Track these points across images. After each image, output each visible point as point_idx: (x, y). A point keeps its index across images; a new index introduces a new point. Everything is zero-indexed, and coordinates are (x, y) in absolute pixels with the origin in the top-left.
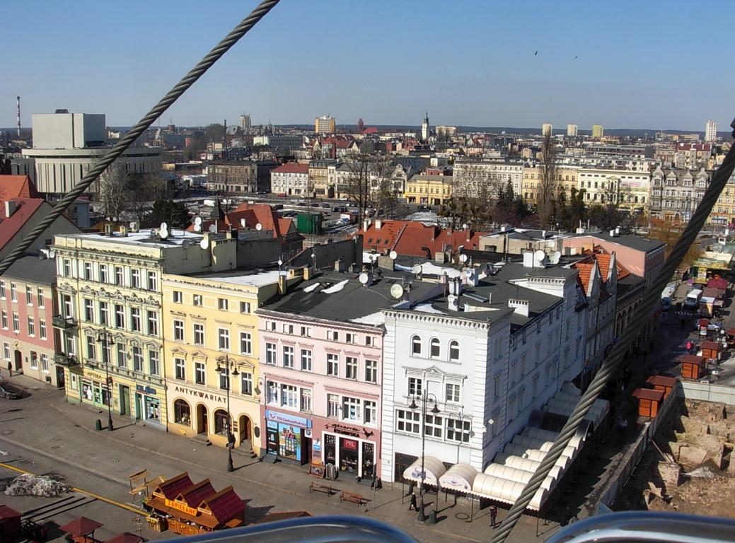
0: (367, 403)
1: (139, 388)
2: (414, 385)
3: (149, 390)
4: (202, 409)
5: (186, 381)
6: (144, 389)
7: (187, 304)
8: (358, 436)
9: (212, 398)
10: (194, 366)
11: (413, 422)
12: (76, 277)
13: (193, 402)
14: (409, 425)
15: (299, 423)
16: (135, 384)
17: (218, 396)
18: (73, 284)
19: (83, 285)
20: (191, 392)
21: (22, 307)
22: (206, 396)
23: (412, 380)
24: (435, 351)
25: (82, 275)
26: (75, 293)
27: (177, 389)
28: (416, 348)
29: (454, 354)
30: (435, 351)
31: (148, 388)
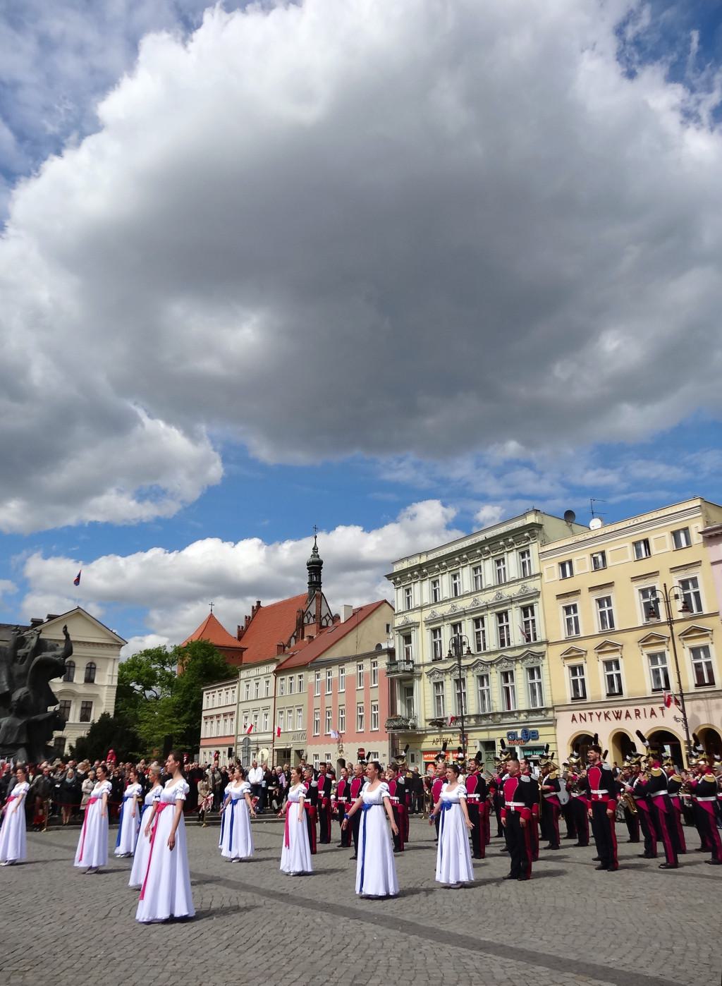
4: (622, 741)
5: (589, 700)
7: (584, 575)
9: (638, 714)
10: (601, 667)
13: (604, 731)
16: (504, 734)
17: (648, 708)
18: (414, 617)
19: (427, 614)
20: (599, 716)
21: (351, 693)
22: (628, 715)
25: (427, 599)
26: (416, 625)
27: (574, 719)
31: (525, 732)
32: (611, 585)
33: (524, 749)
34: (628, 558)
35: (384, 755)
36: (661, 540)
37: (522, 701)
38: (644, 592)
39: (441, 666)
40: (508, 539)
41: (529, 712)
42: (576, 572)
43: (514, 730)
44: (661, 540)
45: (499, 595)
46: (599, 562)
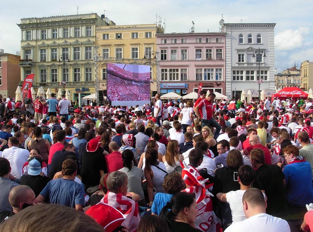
0: (217, 70)
1: (78, 90)
2: (240, 57)
3: (84, 89)
6: (81, 90)
8: (213, 87)
11: (240, 75)
12: (35, 39)
14: (238, 77)
15: (181, 86)
19: (40, 43)
23: (239, 55)
24: (250, 41)
25: (40, 37)
28: (241, 41)
29: (259, 41)
30: (250, 41)
32: (123, 45)
33: (81, 94)
34: (129, 37)
35: (5, 96)
36: (142, 35)
37: (83, 79)
38: (133, 49)
39: (46, 64)
40: (83, 21)
41: (85, 82)
42: (109, 38)
43: (79, 88)
44: (142, 35)
45: (77, 41)
46: (119, 37)
